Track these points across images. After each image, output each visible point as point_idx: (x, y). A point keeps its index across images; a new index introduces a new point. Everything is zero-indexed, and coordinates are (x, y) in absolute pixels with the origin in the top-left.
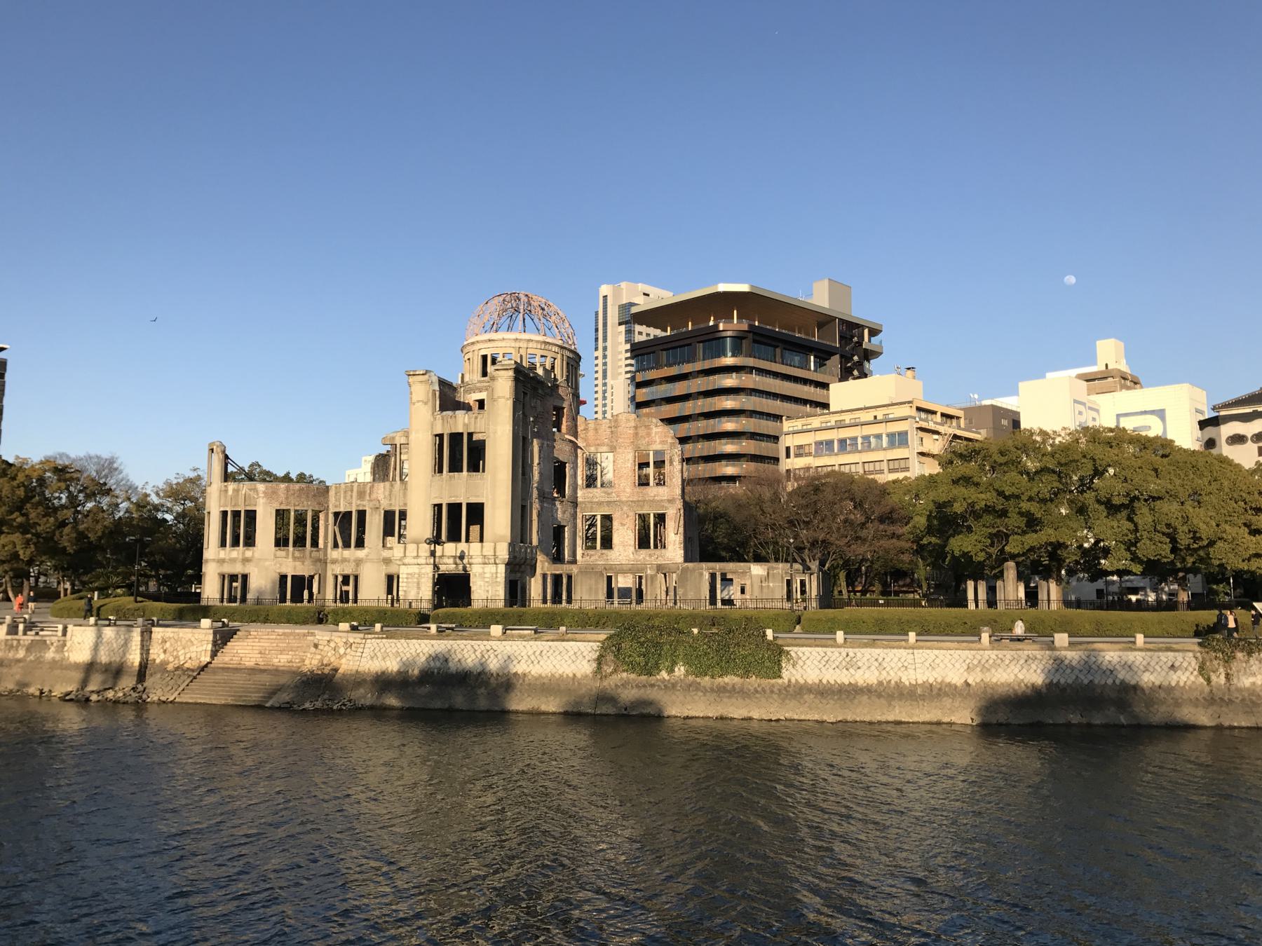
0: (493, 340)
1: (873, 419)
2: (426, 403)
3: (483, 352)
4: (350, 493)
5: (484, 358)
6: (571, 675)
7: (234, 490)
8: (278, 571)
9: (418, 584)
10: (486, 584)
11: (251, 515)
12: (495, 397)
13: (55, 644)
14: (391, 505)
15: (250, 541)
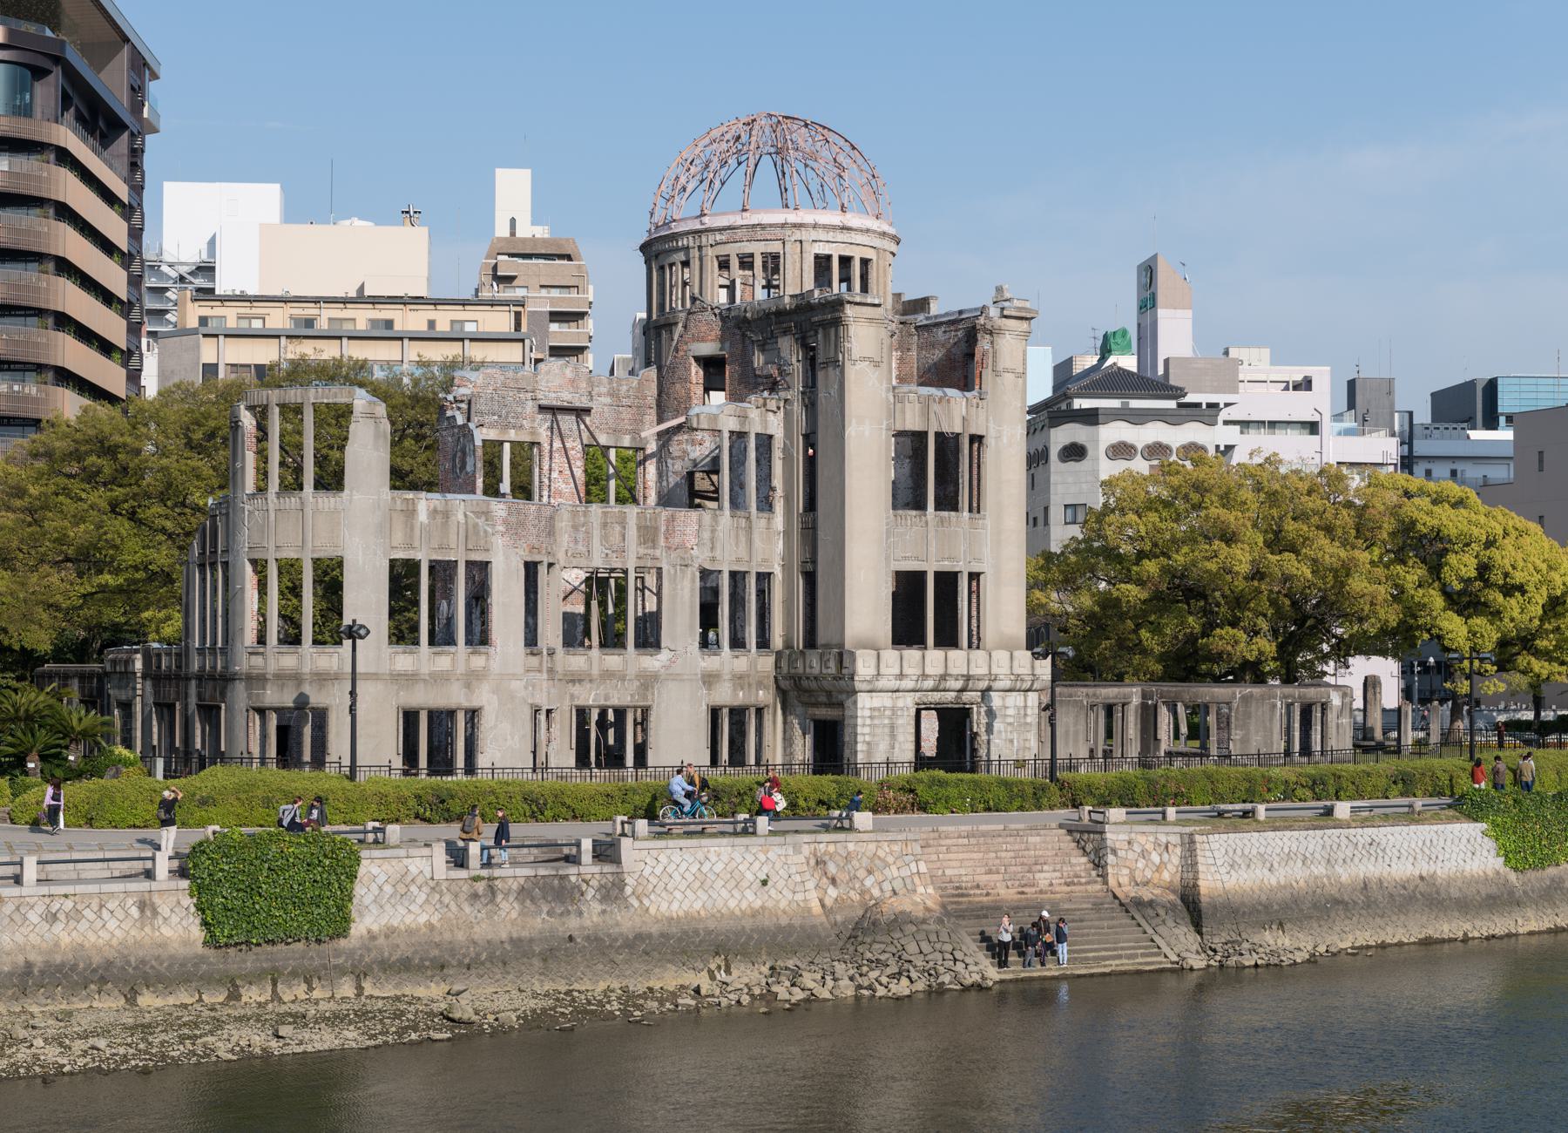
0: (849, 229)
1: (423, 327)
2: (877, 364)
3: (823, 249)
4: (618, 528)
5: (822, 263)
6: (1481, 873)
7: (434, 513)
8: (530, 701)
9: (892, 727)
10: (1009, 728)
11: (480, 573)
12: (1000, 367)
13: (594, 883)
14: (713, 559)
15: (480, 637)
